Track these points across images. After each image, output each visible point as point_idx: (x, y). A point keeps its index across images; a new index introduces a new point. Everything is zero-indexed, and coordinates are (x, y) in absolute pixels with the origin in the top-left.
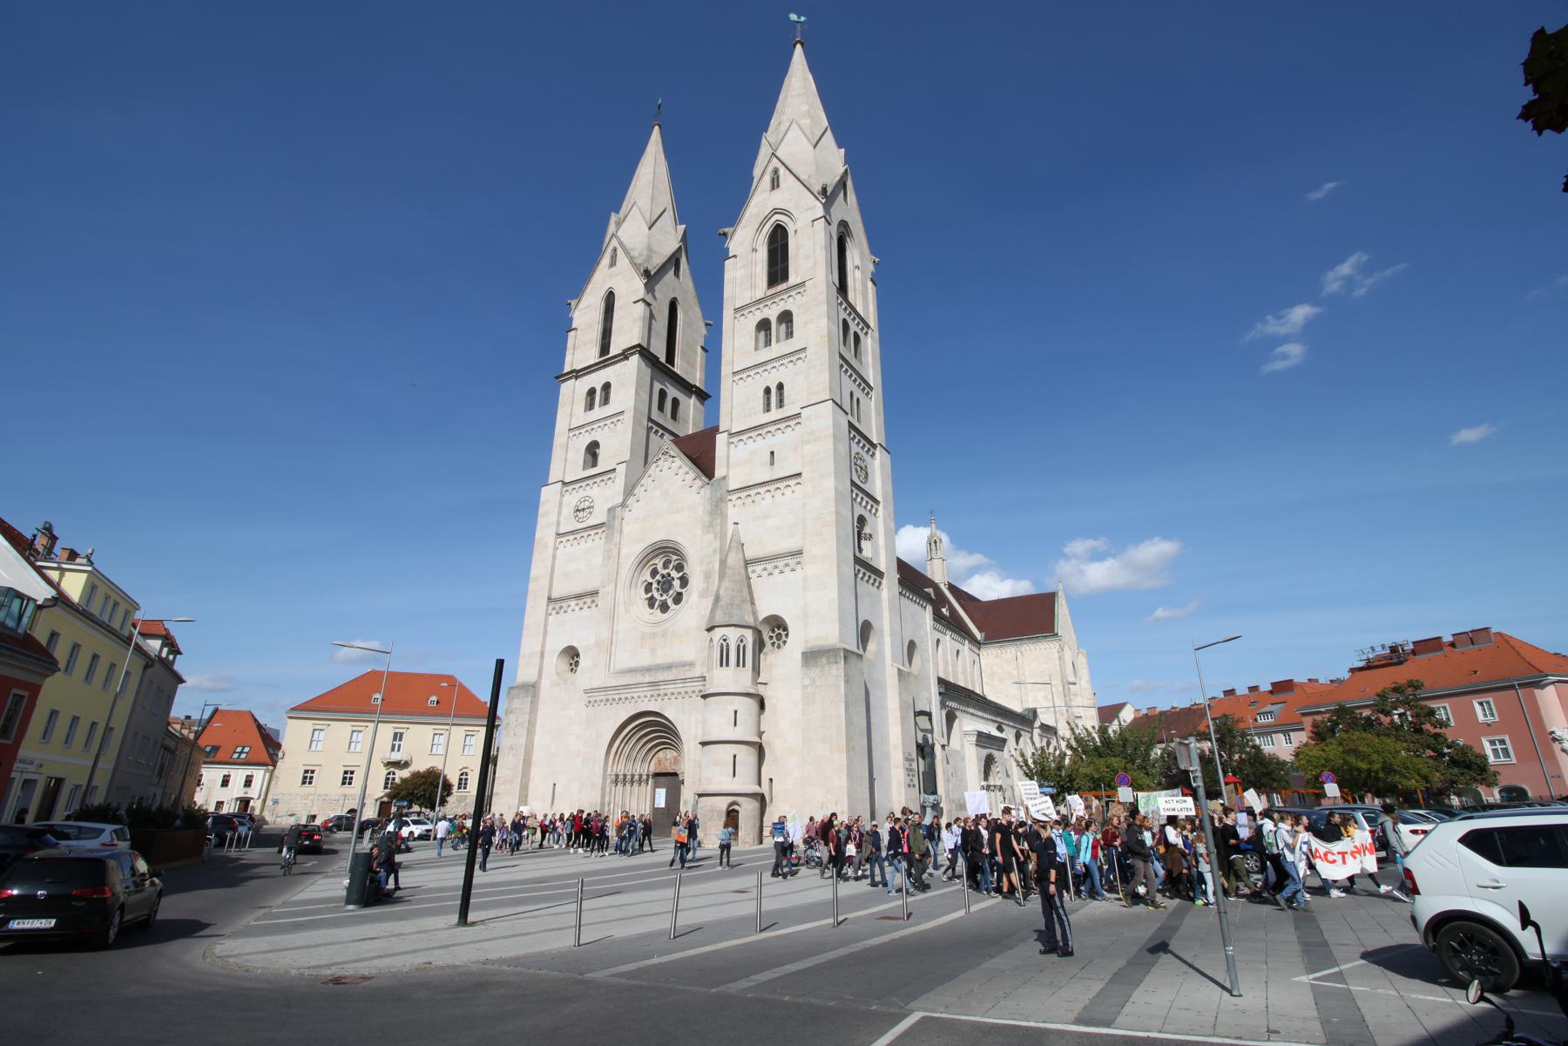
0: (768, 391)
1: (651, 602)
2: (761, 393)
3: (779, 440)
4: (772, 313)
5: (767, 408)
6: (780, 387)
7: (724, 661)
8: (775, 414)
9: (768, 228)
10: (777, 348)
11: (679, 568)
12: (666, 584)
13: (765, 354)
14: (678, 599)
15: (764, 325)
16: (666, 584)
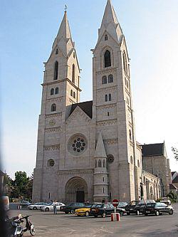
0: (106, 95)
1: (75, 149)
2: (104, 96)
3: (110, 110)
4: (107, 75)
5: (106, 101)
6: (110, 95)
7: (100, 166)
8: (108, 102)
9: (104, 51)
10: (108, 85)
11: (82, 141)
12: (79, 145)
13: (105, 86)
14: (82, 149)
15: (104, 78)
16: (79, 145)
